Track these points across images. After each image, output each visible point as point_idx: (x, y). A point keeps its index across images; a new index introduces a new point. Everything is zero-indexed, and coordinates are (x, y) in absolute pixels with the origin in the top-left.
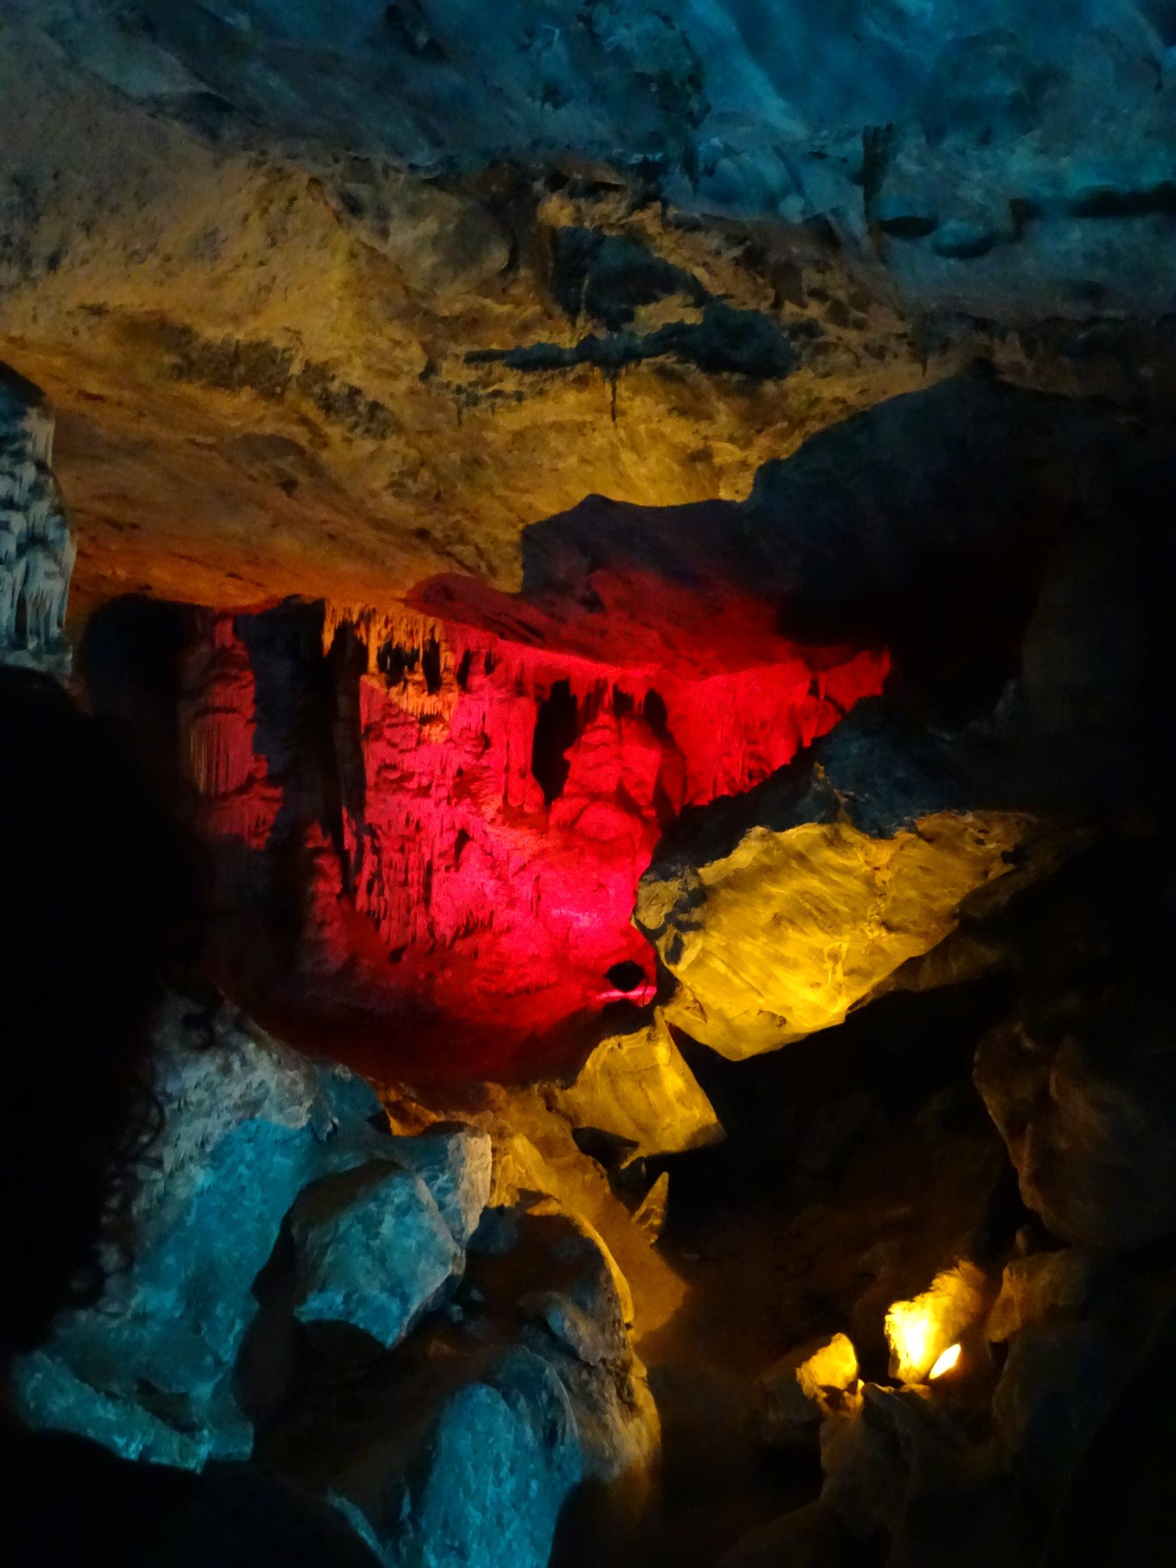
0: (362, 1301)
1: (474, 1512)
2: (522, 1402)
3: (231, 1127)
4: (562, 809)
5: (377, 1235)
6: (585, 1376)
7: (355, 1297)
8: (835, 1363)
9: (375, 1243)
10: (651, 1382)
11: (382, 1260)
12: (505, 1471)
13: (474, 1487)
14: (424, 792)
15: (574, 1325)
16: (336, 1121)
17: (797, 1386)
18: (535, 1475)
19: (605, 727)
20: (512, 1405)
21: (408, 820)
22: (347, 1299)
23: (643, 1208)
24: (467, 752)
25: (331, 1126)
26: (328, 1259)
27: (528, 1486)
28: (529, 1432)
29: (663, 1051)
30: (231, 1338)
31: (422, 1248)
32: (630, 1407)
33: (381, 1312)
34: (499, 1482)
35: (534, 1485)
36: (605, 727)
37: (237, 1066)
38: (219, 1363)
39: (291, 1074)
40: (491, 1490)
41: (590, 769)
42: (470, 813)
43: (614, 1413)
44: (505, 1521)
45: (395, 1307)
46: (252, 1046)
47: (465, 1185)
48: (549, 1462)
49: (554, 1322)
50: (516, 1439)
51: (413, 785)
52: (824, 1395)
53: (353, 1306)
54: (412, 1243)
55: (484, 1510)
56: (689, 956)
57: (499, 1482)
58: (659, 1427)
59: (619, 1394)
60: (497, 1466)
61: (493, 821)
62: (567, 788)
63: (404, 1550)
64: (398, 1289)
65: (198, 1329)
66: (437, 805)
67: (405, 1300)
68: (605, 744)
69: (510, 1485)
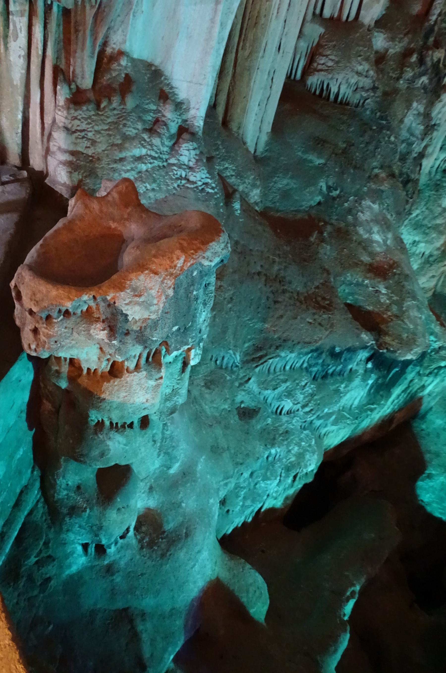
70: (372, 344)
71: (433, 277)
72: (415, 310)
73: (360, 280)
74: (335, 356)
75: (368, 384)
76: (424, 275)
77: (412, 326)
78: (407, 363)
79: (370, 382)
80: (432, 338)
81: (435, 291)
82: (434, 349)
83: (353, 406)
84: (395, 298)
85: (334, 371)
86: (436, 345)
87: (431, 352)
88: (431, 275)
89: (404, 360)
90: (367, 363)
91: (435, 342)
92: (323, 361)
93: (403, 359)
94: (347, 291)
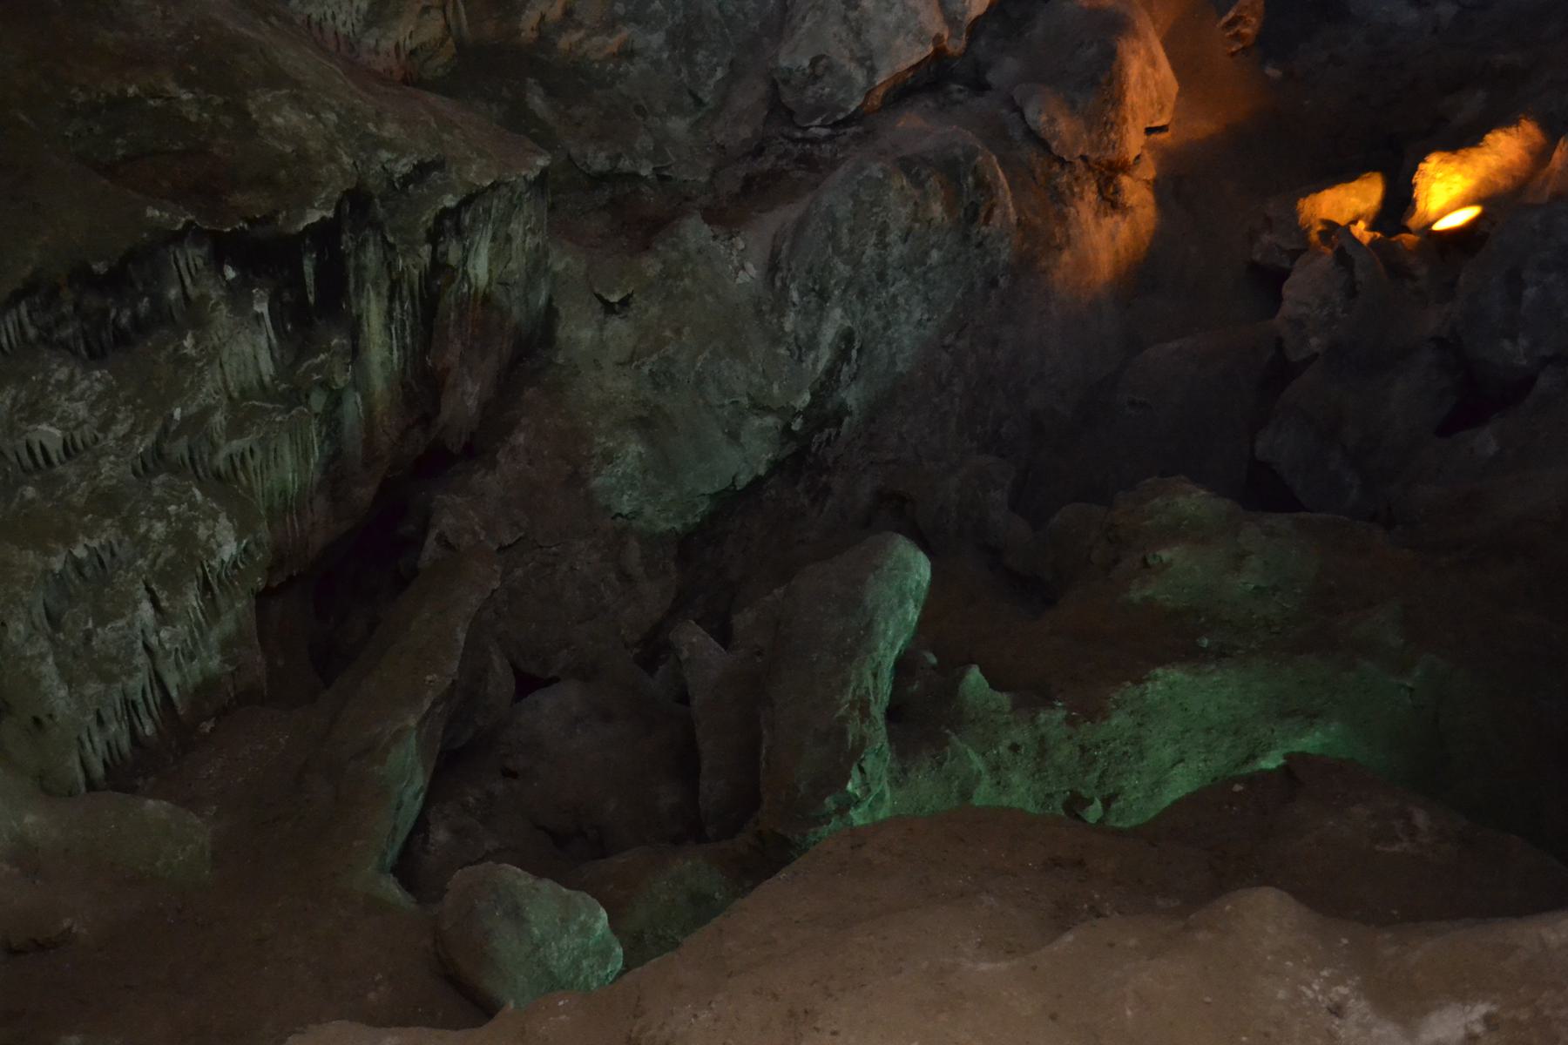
0: (829, 68)
1: (841, 267)
2: (933, 183)
5: (856, 7)
6: (1056, 168)
7: (823, 62)
8: (1351, 202)
9: (853, 15)
10: (1157, 186)
11: (858, 34)
12: (892, 237)
13: (846, 245)
15: (1052, 121)
17: (1294, 214)
18: (940, 249)
20: (919, 183)
22: (814, 62)
23: (1231, 14)
26: (807, 24)
27: (926, 253)
28: (937, 209)
30: (712, 82)
31: (901, 25)
32: (1111, 202)
33: (848, 80)
34: (883, 245)
35: (935, 255)
38: (699, 102)
40: (870, 252)
43: (1085, 207)
44: (890, 279)
45: (860, 77)
48: (966, 238)
49: (1030, 113)
50: (915, 213)
52: (1319, 228)
53: (819, 70)
54: (891, 19)
55: (857, 265)
57: (883, 245)
58: (1152, 226)
59: (1100, 191)
60: (883, 231)
63: (778, 284)
64: (867, 61)
65: (678, 72)
67: (872, 71)
69: (897, 251)
70: (189, 224)
71: (426, 10)
72: (287, 107)
73: (114, 92)
74: (116, 282)
75: (259, 317)
76: (398, 14)
77: (289, 149)
78: (325, 233)
79: (262, 308)
80: (385, 155)
81: (460, 44)
82: (407, 179)
83: (267, 379)
84: (218, 100)
85: (135, 317)
86: (403, 167)
87: (405, 185)
88: (418, 7)
89: (306, 228)
90: (221, 272)
91: (396, 161)
92: (77, 306)
93: (301, 227)
94: (98, 129)
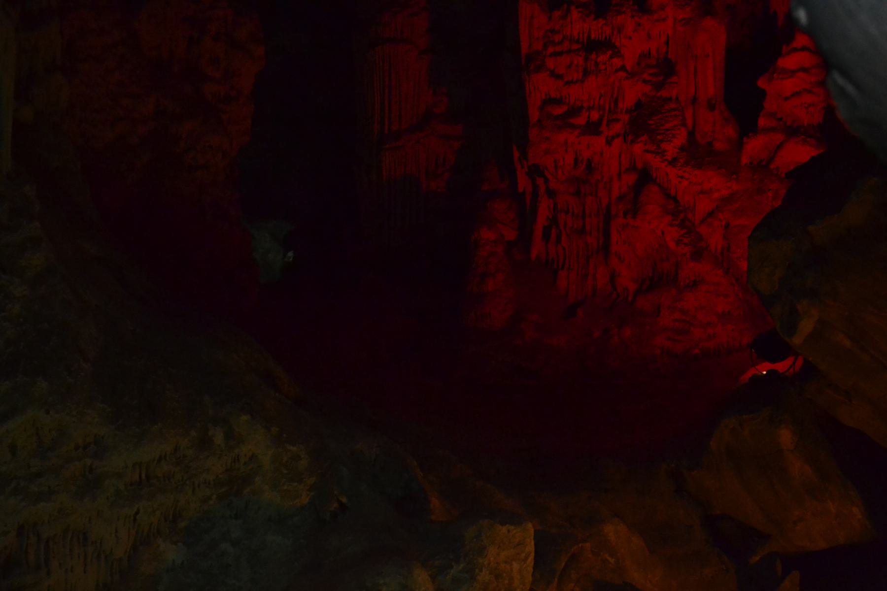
3: (211, 502)
4: (754, 146)
14: (593, 128)
16: (344, 500)
19: (804, 49)
21: (576, 160)
24: (645, 81)
25: (336, 505)
29: (786, 436)
36: (804, 49)
37: (219, 437)
39: (294, 449)
41: (786, 99)
42: (647, 151)
46: (245, 418)
47: (484, 576)
51: (581, 120)
56: (806, 326)
61: (673, 162)
62: (762, 122)
66: (609, 142)
68: (804, 70)
